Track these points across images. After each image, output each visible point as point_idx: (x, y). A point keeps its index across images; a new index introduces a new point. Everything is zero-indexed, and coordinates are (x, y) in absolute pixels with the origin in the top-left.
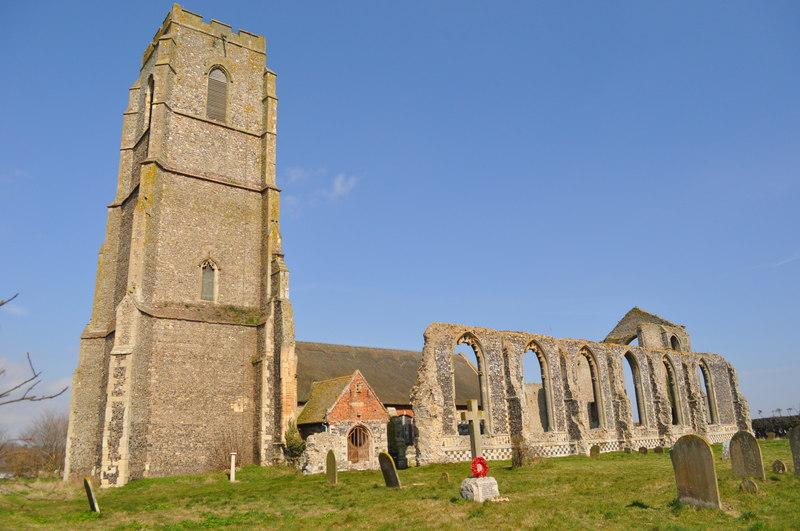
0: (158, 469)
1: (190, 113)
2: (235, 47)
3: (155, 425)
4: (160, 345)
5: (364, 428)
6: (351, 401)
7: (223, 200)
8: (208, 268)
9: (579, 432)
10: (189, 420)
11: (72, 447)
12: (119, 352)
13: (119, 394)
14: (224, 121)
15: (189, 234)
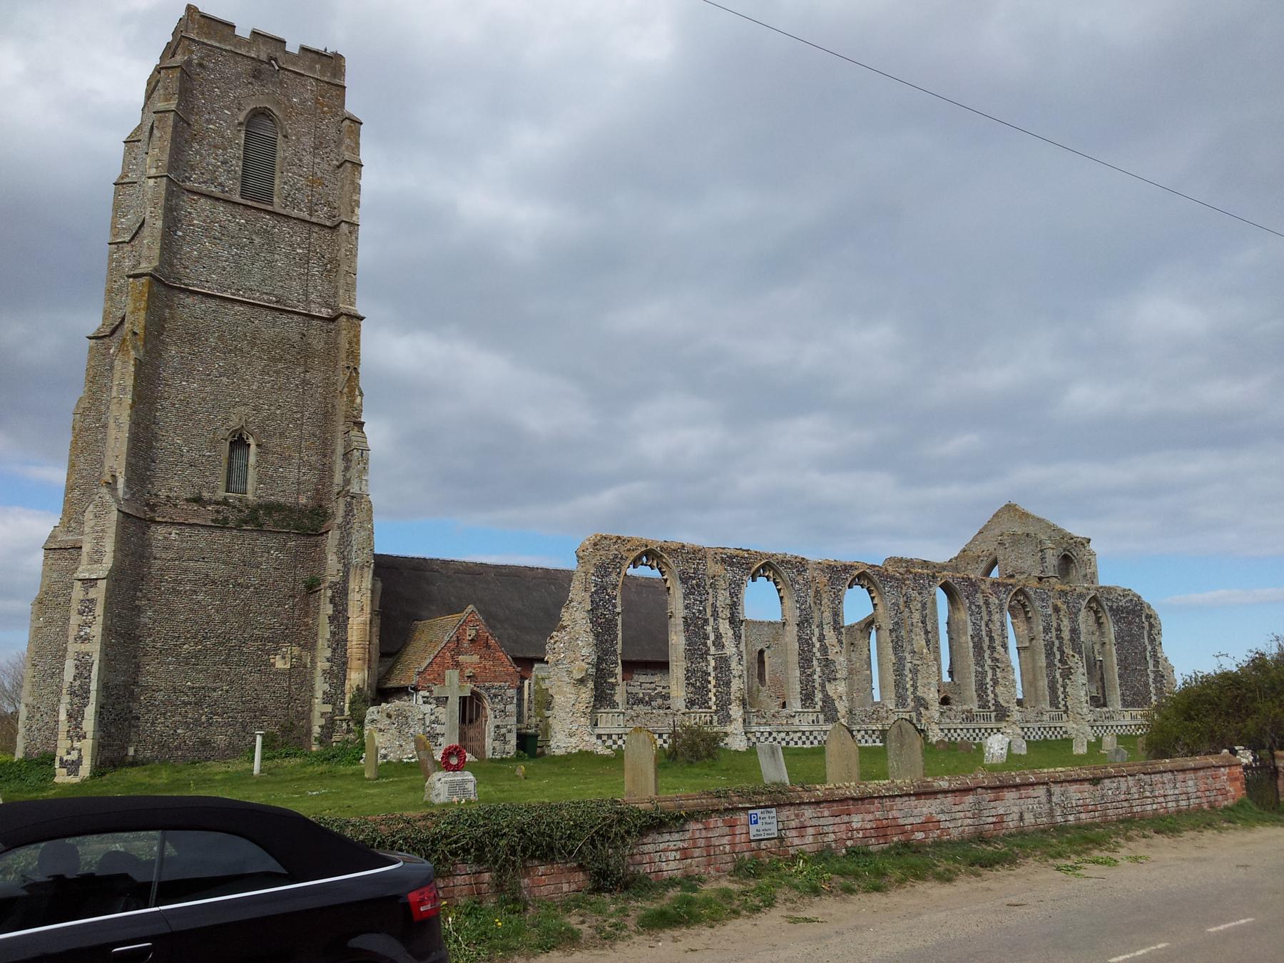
2: (292, 76)
6: (459, 654)
7: (268, 333)
9: (836, 711)
10: (200, 680)
11: (28, 718)
12: (87, 576)
13: (85, 639)
14: (271, 203)
15: (208, 389)
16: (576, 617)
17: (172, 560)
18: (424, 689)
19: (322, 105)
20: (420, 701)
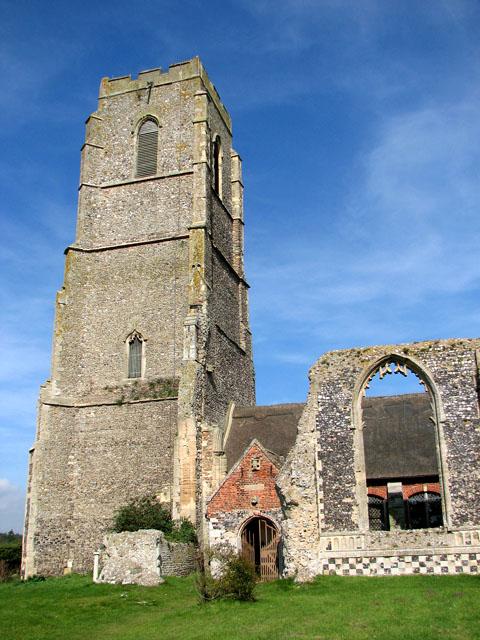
0: (80, 566)
1: (118, 182)
3: (78, 520)
4: (82, 435)
5: (270, 523)
6: (244, 483)
7: (148, 261)
8: (136, 341)
16: (309, 439)
17: (91, 431)
18: (212, 516)
19: (185, 95)
20: (211, 527)
